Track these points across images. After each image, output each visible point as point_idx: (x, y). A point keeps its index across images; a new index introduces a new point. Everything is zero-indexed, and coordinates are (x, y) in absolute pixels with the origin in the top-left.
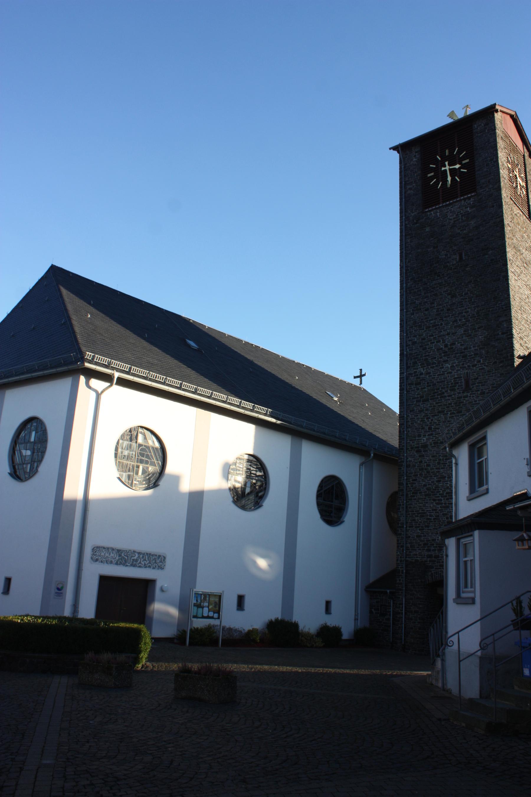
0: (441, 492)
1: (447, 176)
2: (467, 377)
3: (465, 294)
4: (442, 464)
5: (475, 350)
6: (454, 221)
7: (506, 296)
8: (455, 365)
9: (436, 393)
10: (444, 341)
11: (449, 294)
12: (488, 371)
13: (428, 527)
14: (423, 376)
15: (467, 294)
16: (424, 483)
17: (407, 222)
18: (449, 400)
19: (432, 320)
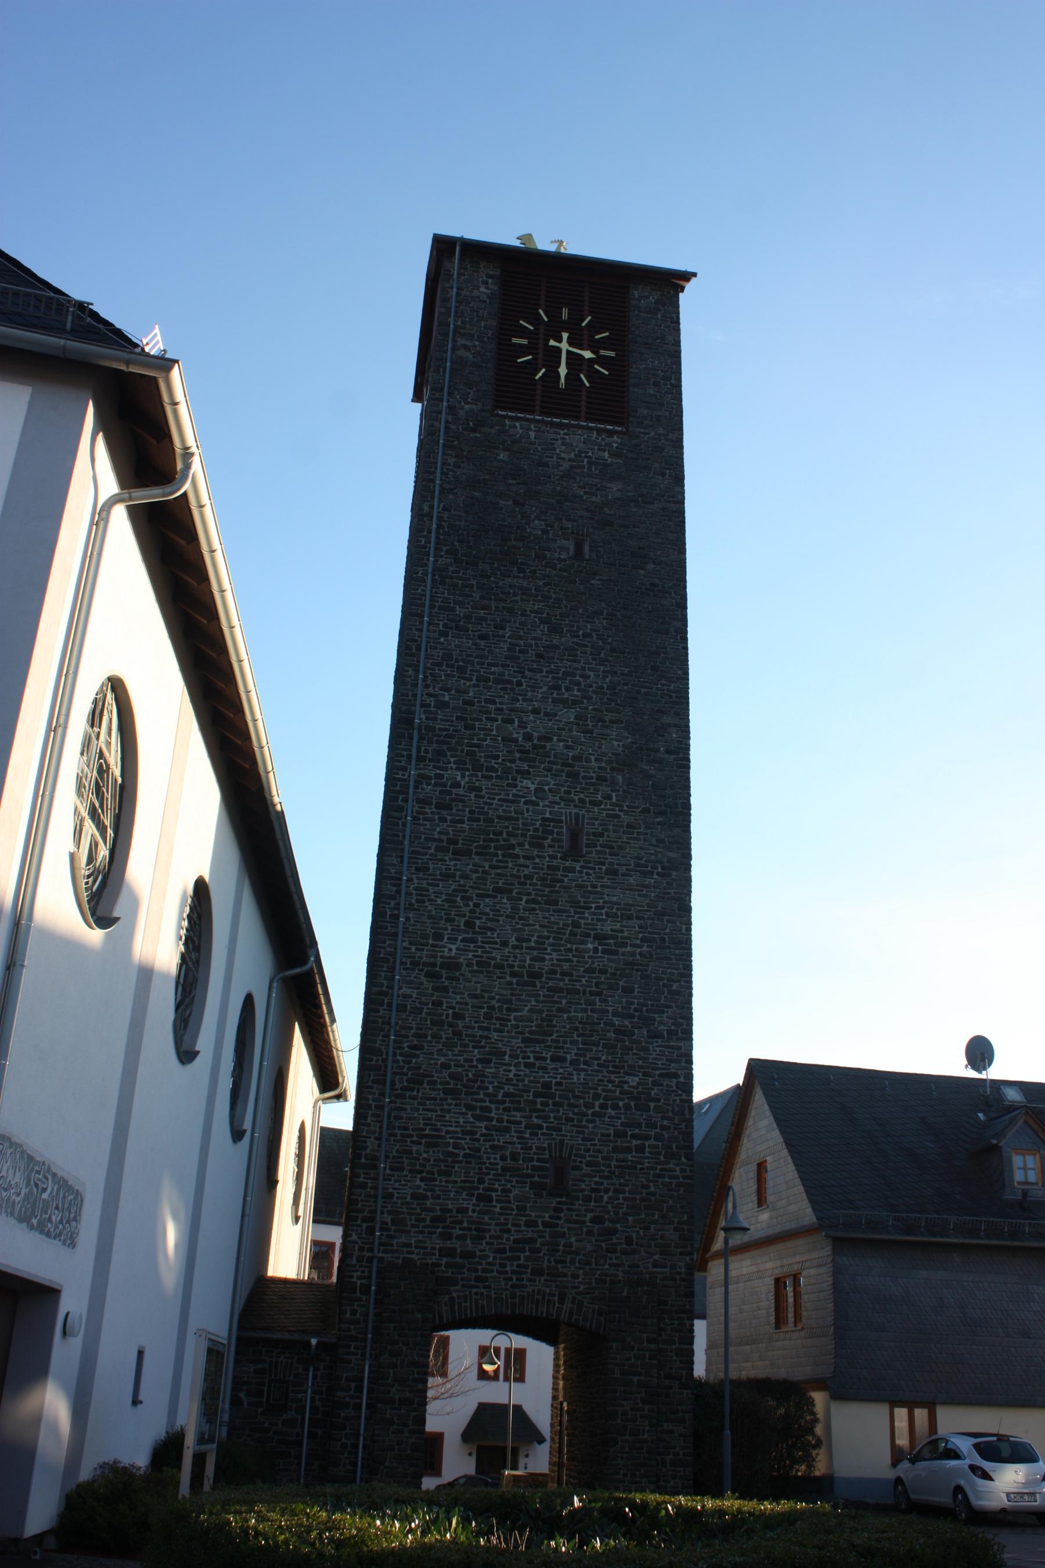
0: (491, 1090)
1: (559, 363)
2: (577, 824)
3: (585, 636)
4: (497, 1019)
5: (599, 768)
6: (572, 467)
7: (680, 672)
8: (546, 788)
9: (492, 840)
10: (523, 725)
11: (543, 621)
12: (629, 826)
13: (448, 1174)
14: (461, 791)
15: (590, 636)
16: (443, 1059)
17: (450, 418)
18: (526, 866)
19: (496, 665)
